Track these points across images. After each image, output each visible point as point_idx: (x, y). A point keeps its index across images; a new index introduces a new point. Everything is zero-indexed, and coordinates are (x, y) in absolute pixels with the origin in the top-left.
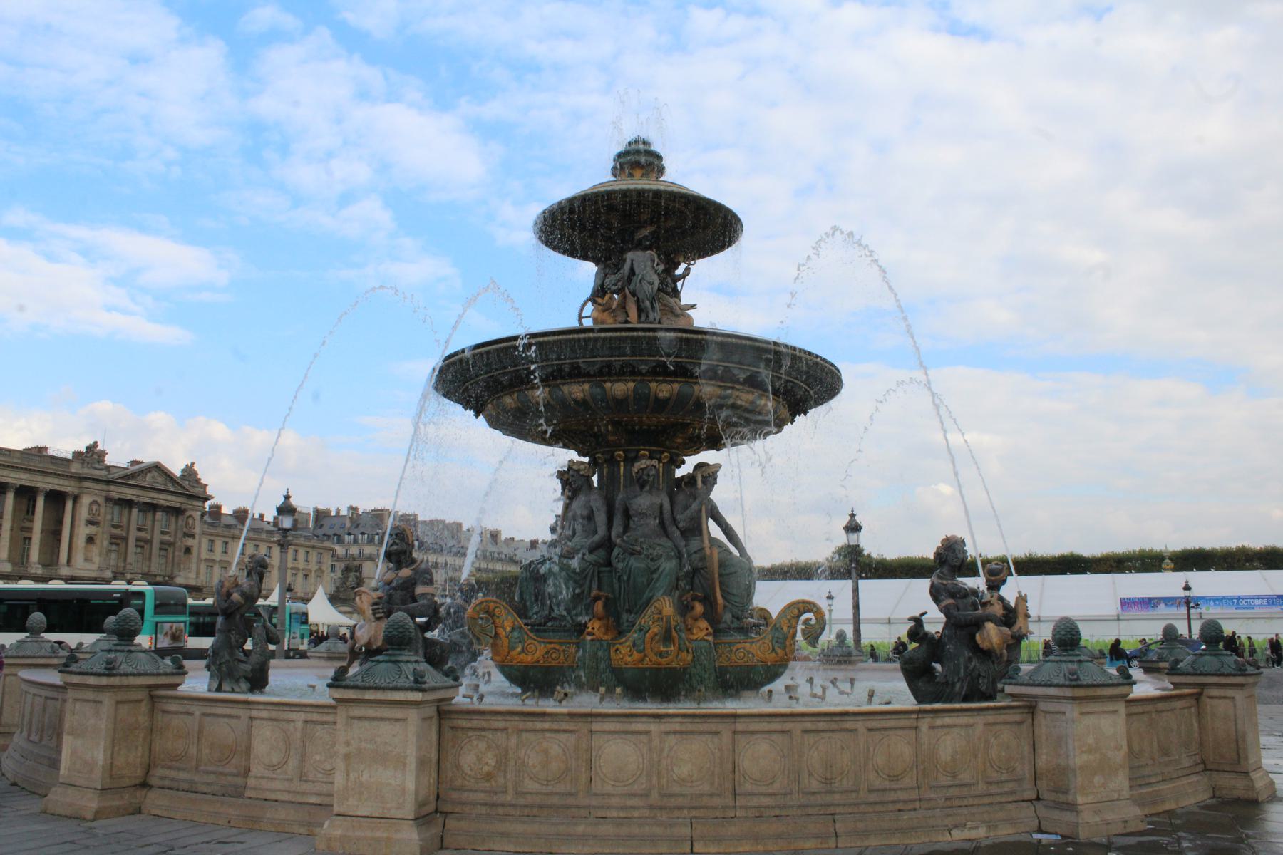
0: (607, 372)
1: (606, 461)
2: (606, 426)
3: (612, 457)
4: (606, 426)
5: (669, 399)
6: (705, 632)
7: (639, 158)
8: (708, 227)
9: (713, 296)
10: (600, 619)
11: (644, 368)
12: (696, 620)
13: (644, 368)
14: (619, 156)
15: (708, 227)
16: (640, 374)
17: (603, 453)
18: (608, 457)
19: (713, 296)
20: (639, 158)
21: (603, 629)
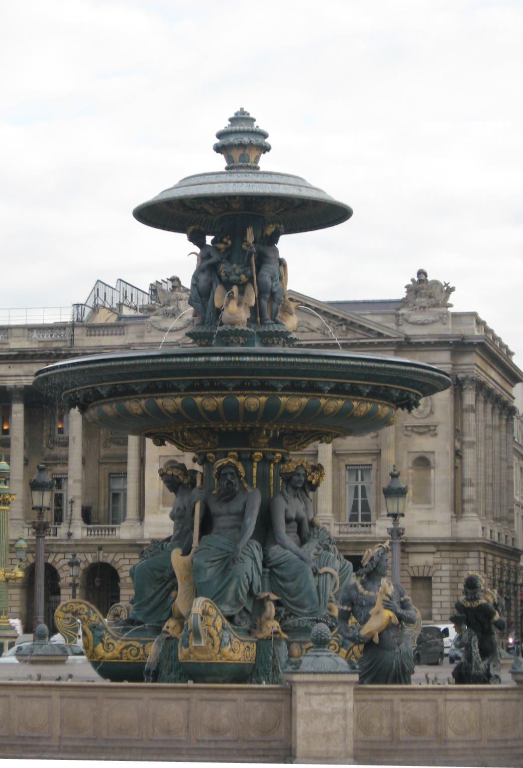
4: (182, 432)
12: (268, 619)
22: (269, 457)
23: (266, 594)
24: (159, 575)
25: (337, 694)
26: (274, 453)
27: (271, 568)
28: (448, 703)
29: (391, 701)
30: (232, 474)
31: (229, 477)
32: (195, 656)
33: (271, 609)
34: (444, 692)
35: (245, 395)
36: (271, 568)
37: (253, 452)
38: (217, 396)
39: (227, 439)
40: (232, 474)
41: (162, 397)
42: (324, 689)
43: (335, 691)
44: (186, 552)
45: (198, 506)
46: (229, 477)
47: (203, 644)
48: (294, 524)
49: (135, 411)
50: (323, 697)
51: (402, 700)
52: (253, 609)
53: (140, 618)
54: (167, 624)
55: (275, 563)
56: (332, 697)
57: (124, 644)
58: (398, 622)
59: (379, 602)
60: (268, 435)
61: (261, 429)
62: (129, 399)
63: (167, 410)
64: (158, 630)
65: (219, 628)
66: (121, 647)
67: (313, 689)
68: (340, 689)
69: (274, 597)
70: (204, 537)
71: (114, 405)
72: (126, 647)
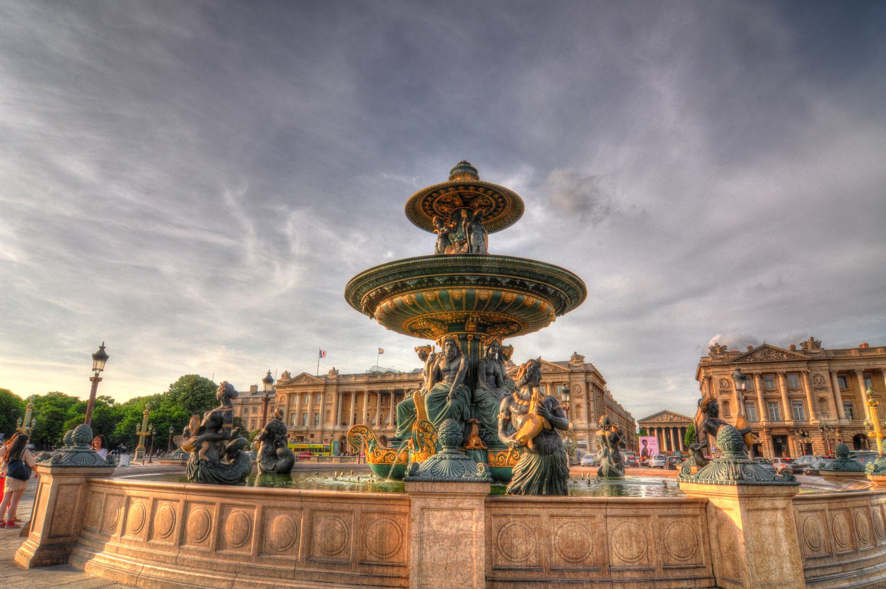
14: (451, 172)
25: (463, 509)
28: (609, 520)
29: (538, 516)
34: (604, 506)
36: (476, 403)
42: (447, 503)
43: (460, 506)
48: (492, 377)
50: (445, 513)
51: (552, 516)
56: (457, 513)
58: (550, 427)
60: (472, 321)
67: (432, 502)
68: (466, 504)
69: (477, 421)
72: (388, 455)
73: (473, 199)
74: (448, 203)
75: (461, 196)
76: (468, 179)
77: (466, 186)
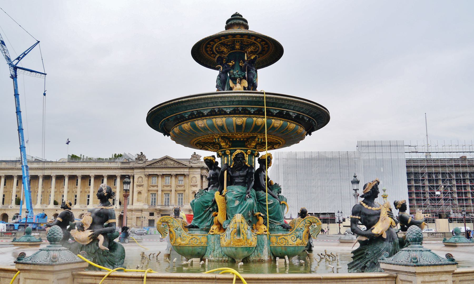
0: (213, 114)
1: (223, 154)
2: (218, 139)
3: (225, 153)
4: (218, 139)
5: (242, 125)
6: (264, 230)
7: (237, 20)
8: (270, 51)
9: (270, 80)
10: (216, 225)
11: (228, 111)
13: (228, 111)
15: (270, 51)
16: (225, 113)
17: (221, 151)
18: (223, 153)
19: (270, 80)
20: (237, 20)
21: (218, 229)
22: (253, 152)
23: (258, 213)
24: (206, 205)
26: (255, 151)
27: (259, 201)
30: (242, 157)
31: (241, 159)
32: (234, 244)
33: (261, 220)
35: (256, 117)
37: (247, 150)
38: (243, 117)
39: (235, 144)
40: (242, 157)
41: (216, 118)
43: (441, 279)
44: (221, 194)
45: (226, 172)
46: (241, 159)
47: (242, 238)
49: (200, 126)
52: (252, 220)
53: (196, 224)
54: (212, 228)
55: (262, 198)
57: (191, 237)
59: (384, 213)
60: (258, 141)
61: (255, 137)
62: (198, 120)
63: (217, 125)
64: (207, 230)
65: (246, 229)
66: (190, 238)
68: (444, 277)
70: (228, 187)
71: (189, 123)
73: (247, 45)
74: (227, 45)
75: (242, 42)
76: (242, 31)
77: (242, 35)
